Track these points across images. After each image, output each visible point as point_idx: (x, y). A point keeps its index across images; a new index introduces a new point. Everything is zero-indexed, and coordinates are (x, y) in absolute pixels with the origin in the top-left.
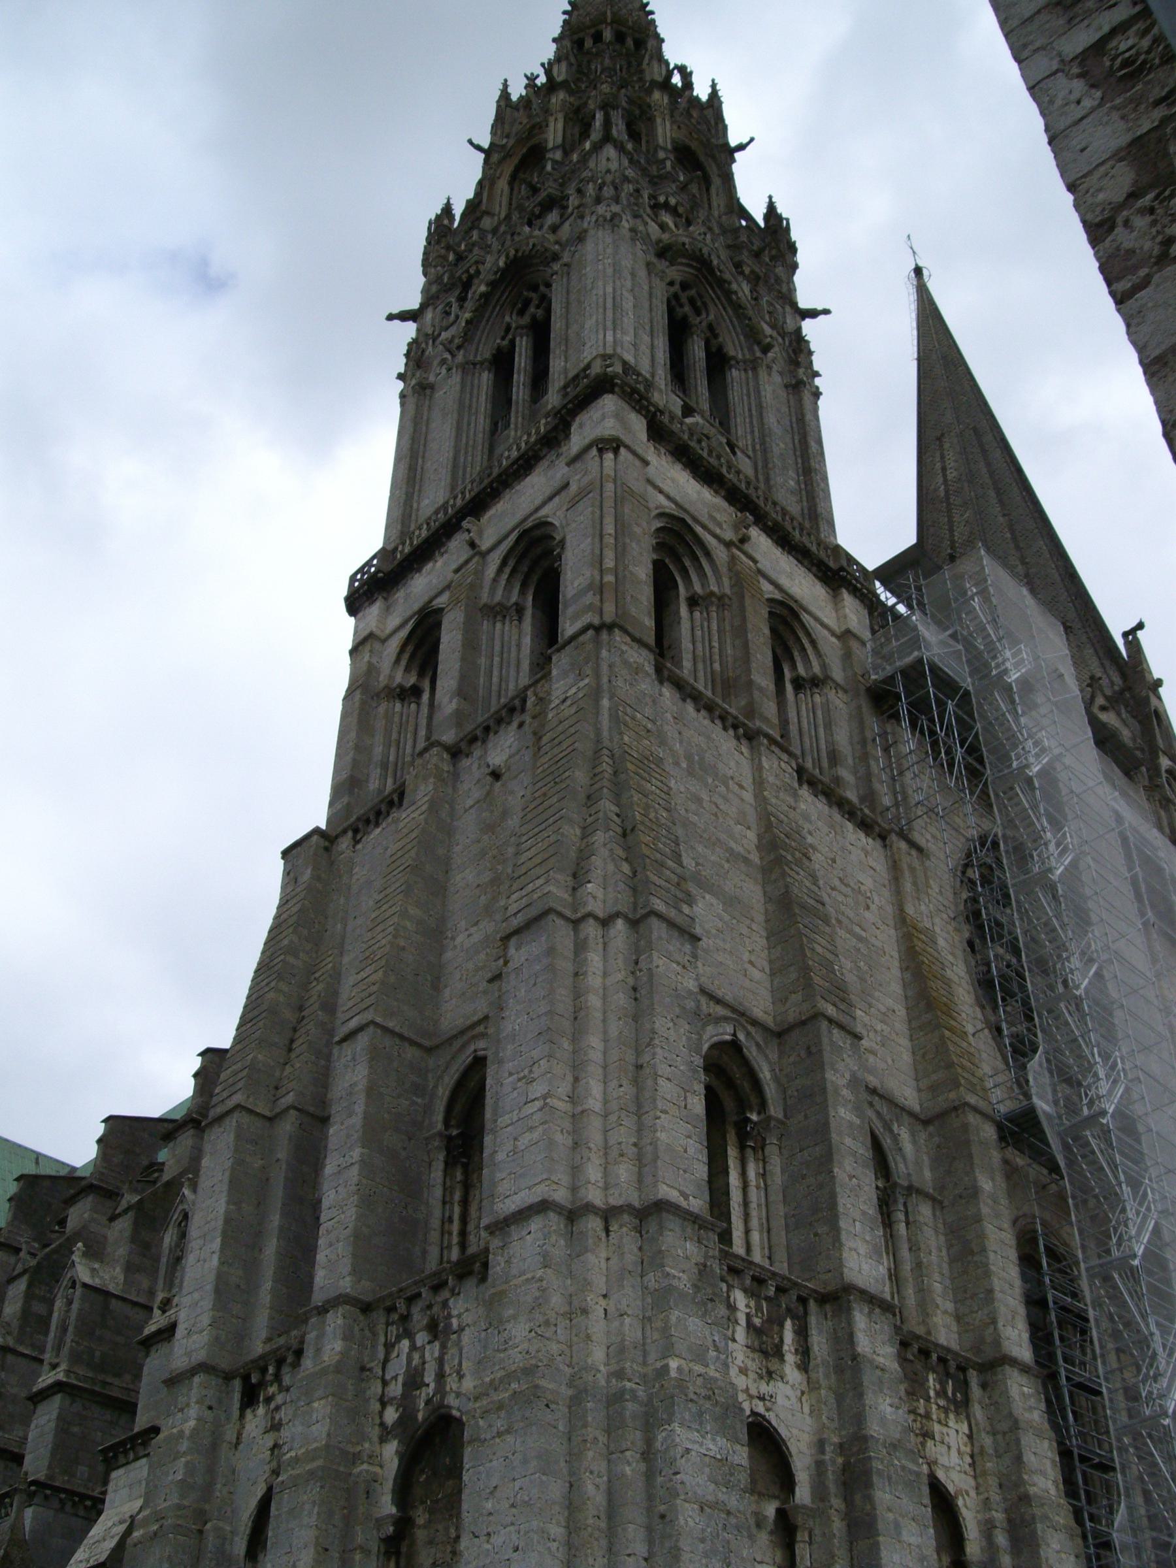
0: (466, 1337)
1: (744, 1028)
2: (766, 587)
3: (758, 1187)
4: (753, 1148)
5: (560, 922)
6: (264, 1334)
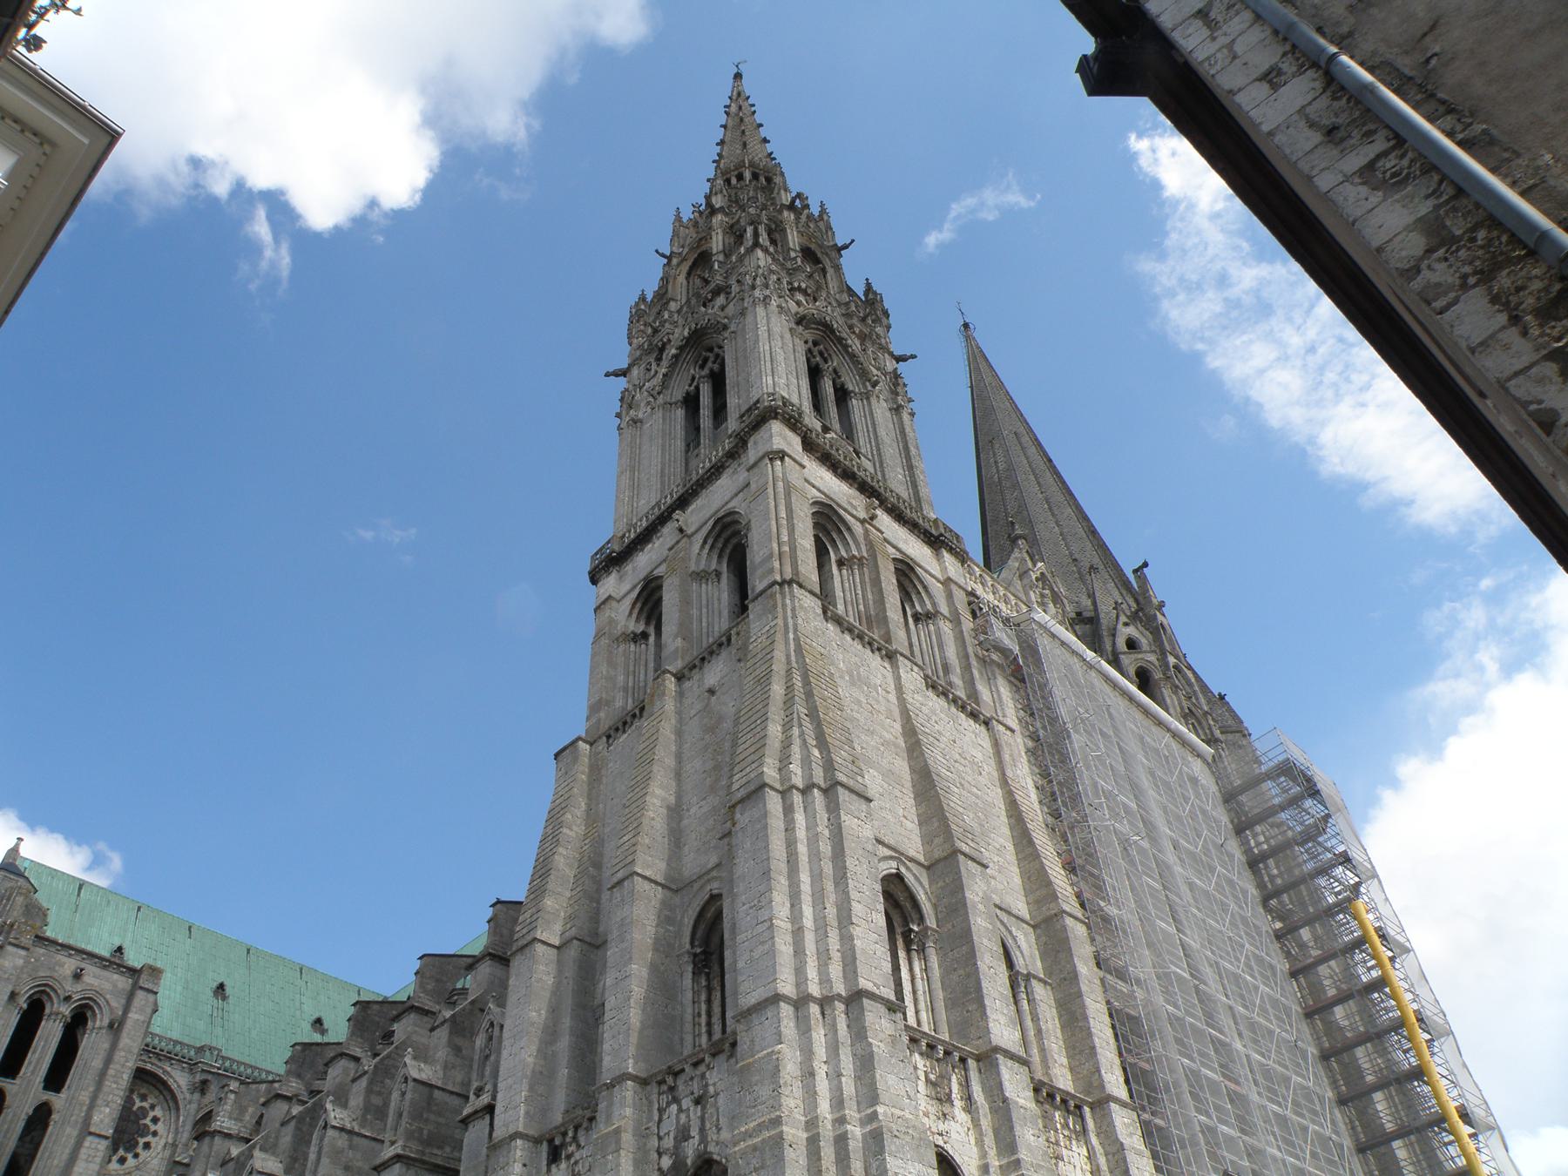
0: (721, 1100)
2: (891, 550)
5: (772, 793)
6: (562, 1108)
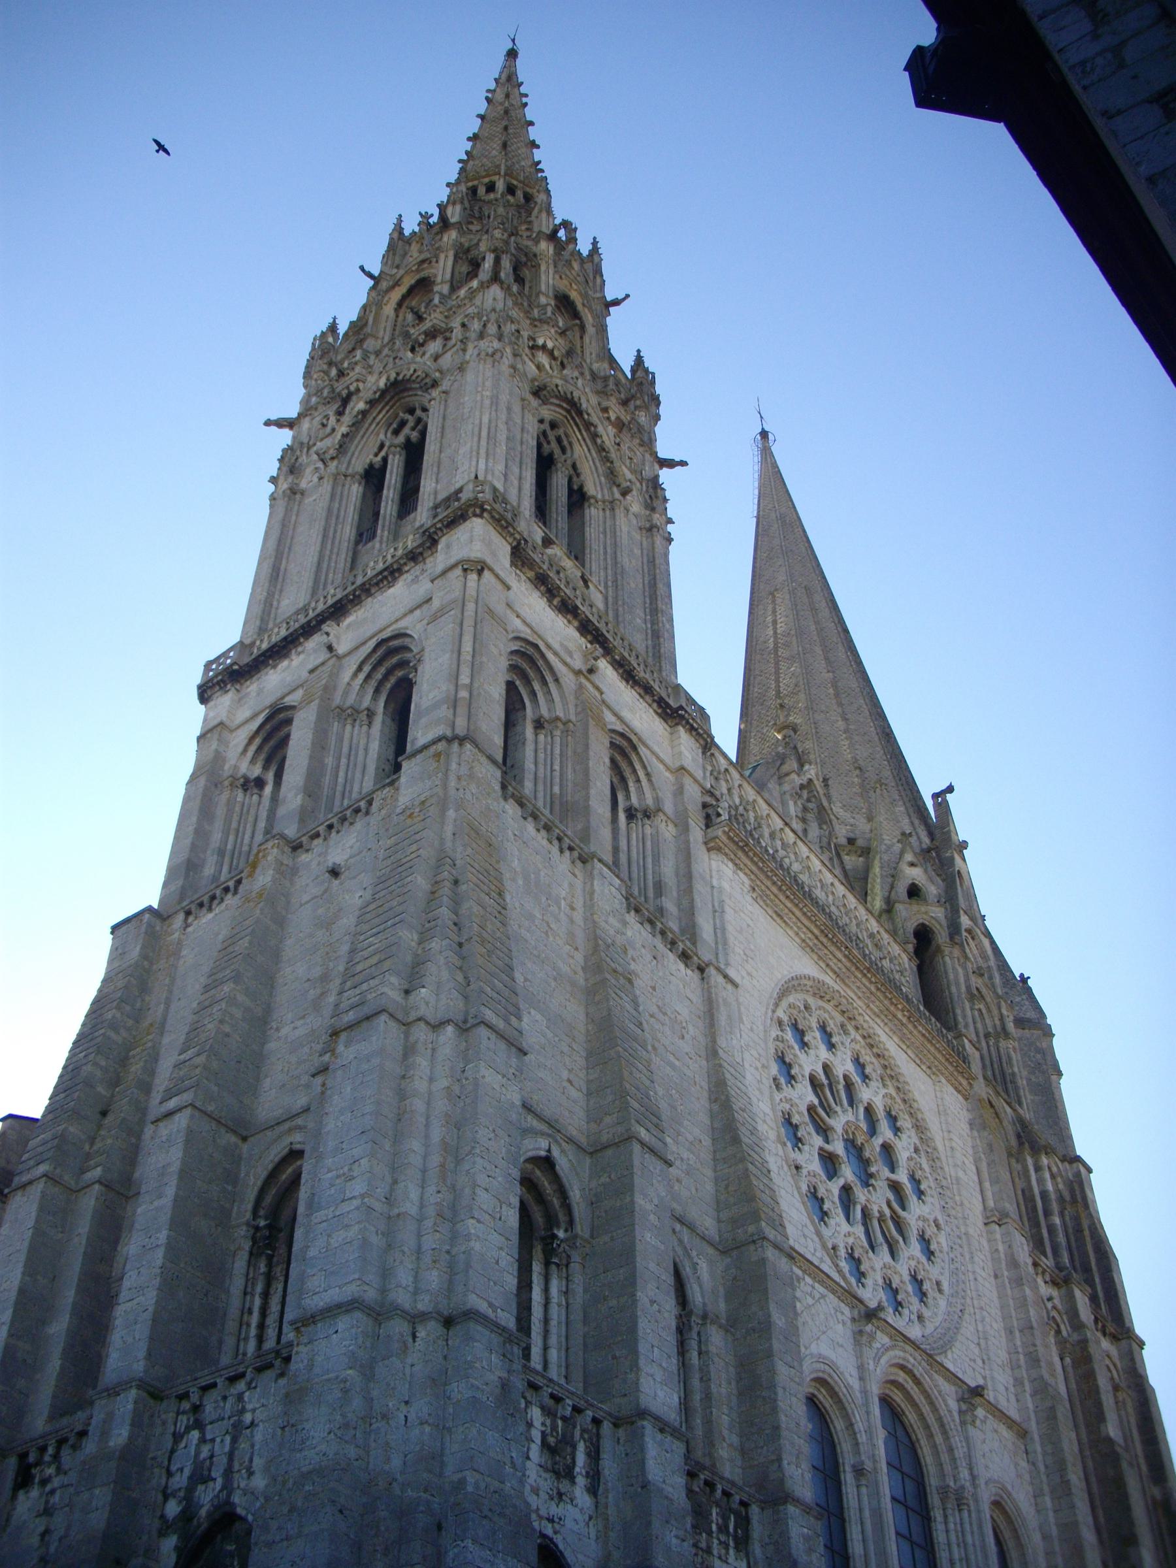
3: (559, 1305)
4: (558, 1265)
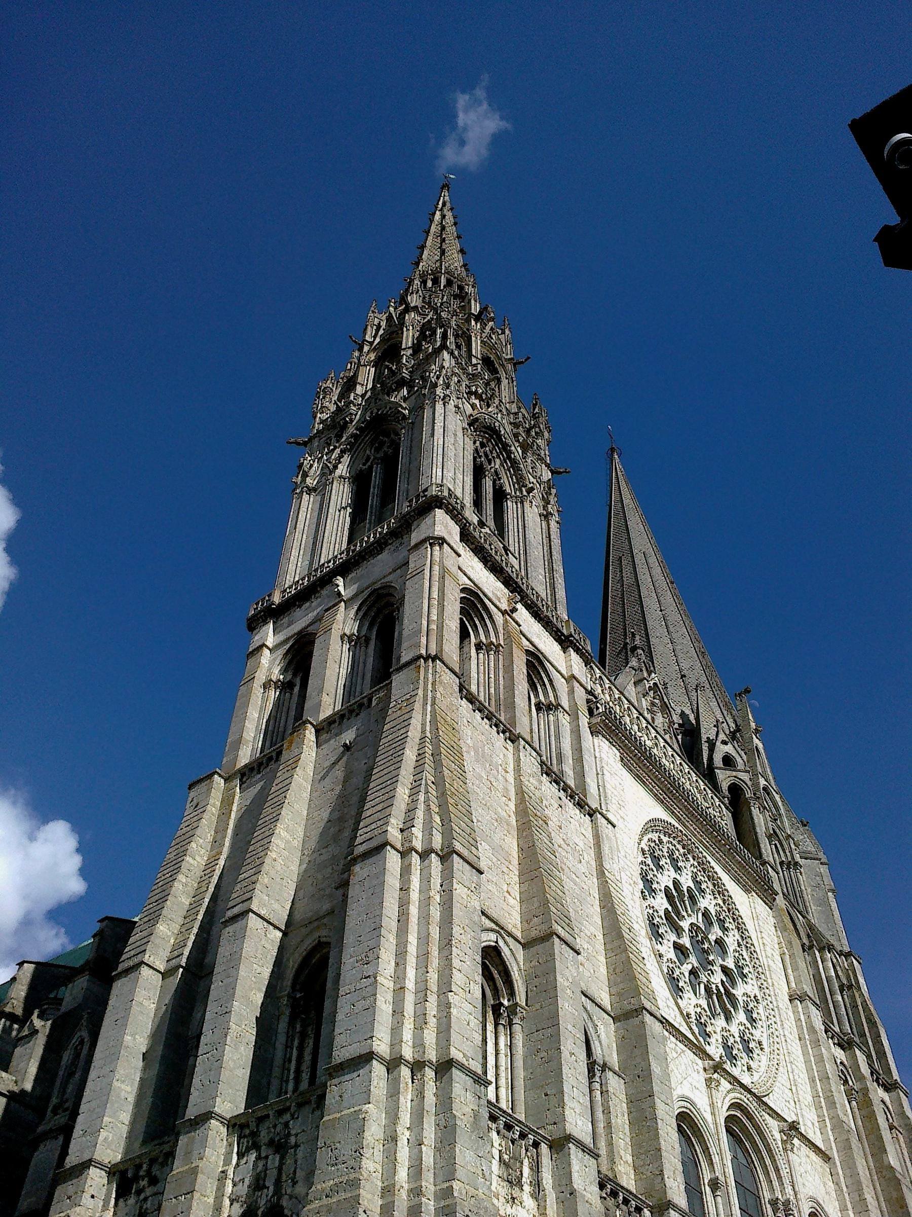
1: (503, 938)
2: (525, 643)
5: (393, 852)
